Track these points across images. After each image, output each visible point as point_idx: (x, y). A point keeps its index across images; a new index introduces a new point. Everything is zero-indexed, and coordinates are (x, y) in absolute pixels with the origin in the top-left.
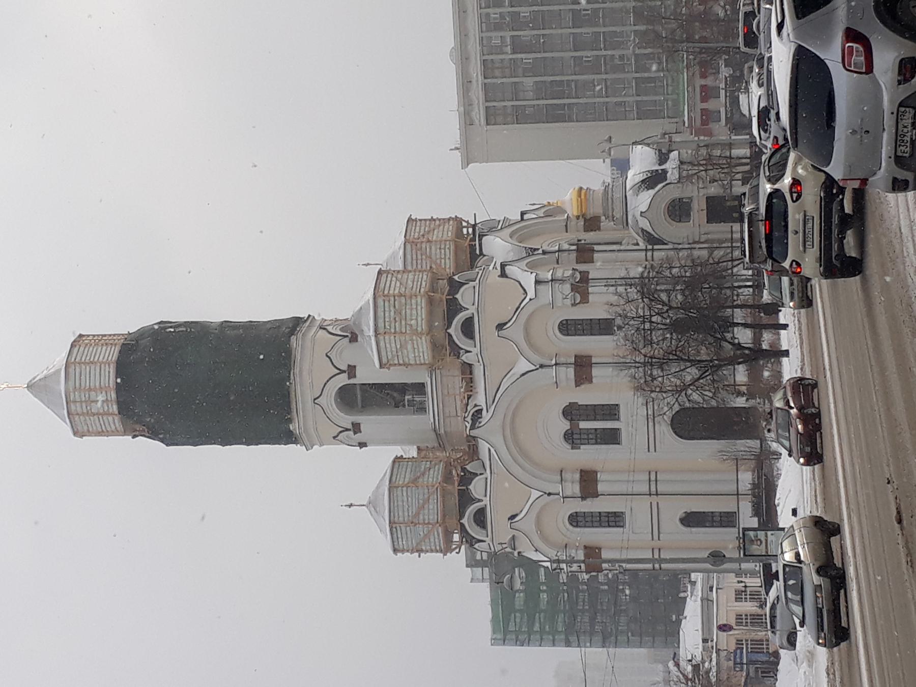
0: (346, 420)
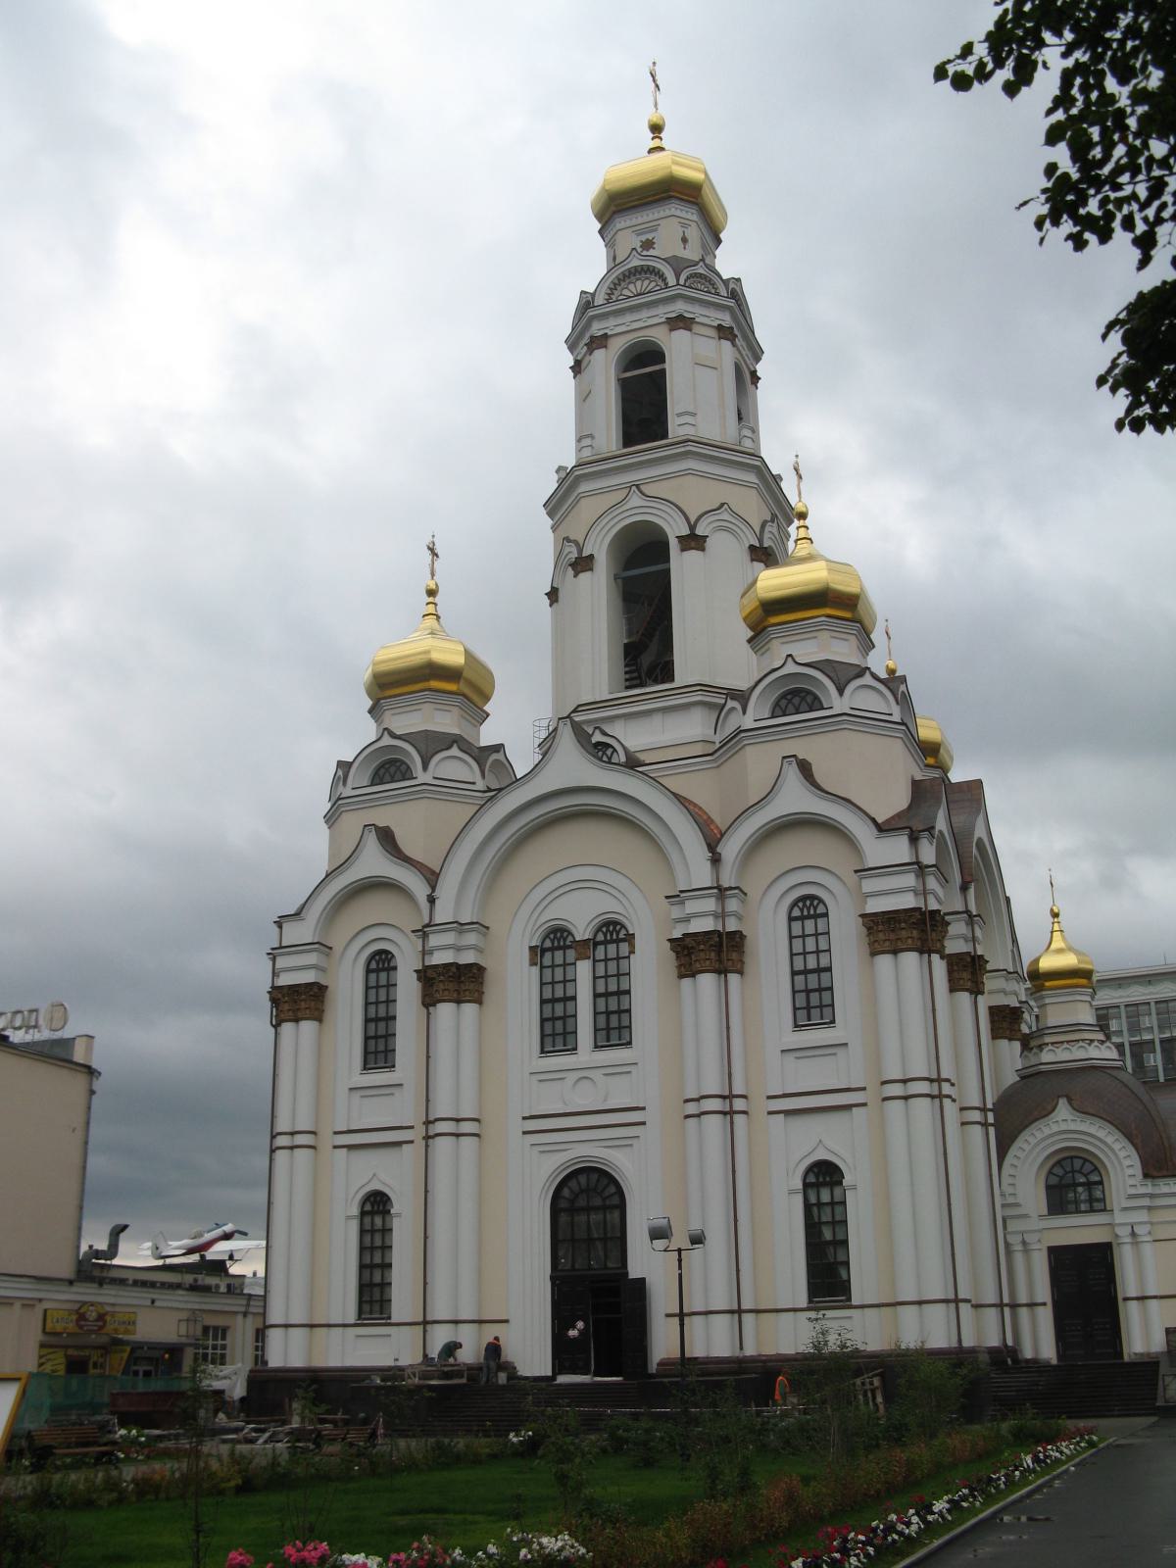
0: (600, 548)
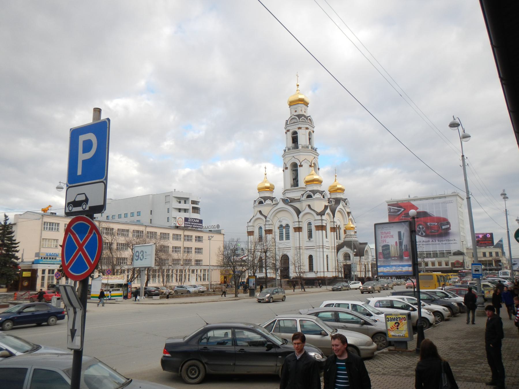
0: (289, 166)
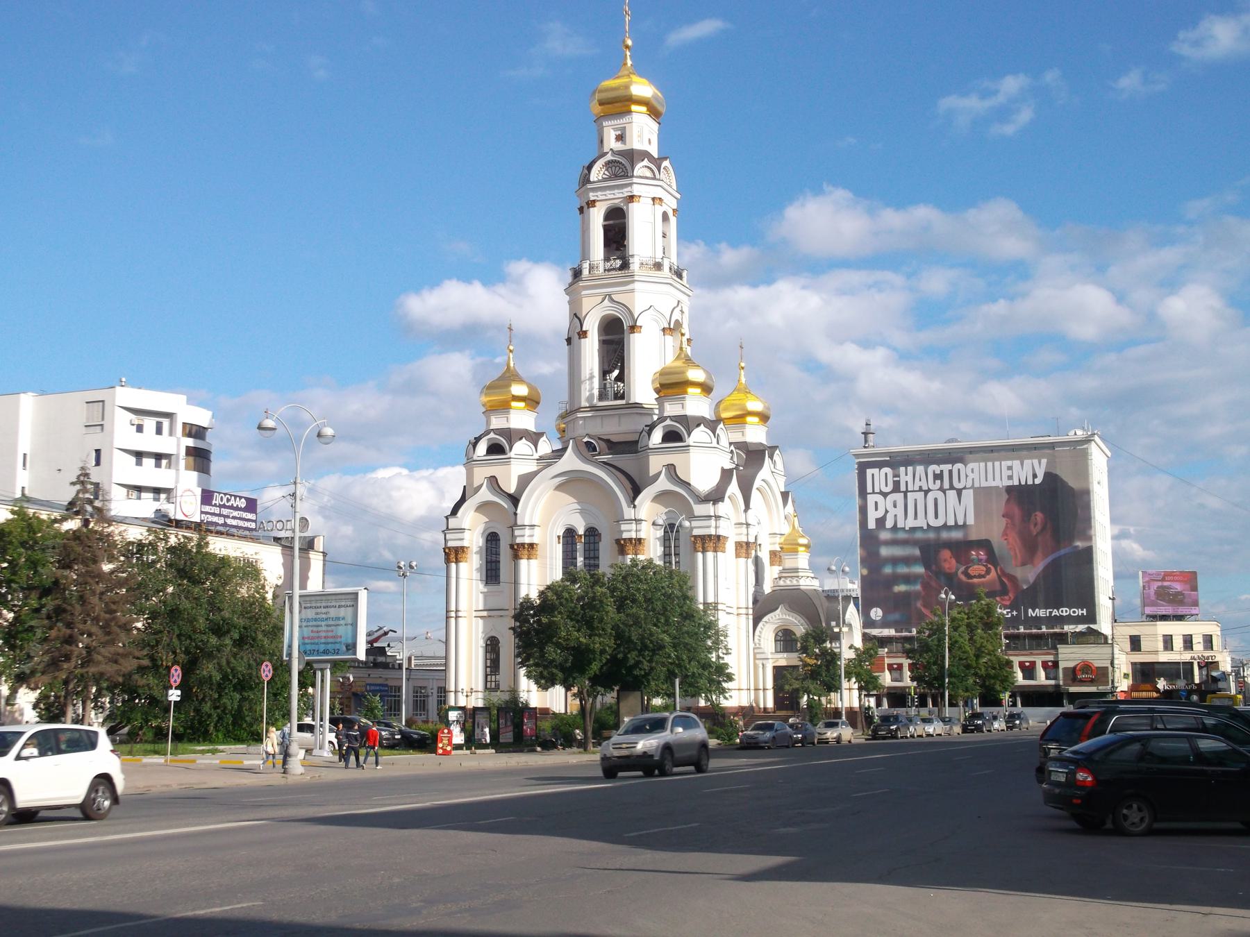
0: (592, 325)
